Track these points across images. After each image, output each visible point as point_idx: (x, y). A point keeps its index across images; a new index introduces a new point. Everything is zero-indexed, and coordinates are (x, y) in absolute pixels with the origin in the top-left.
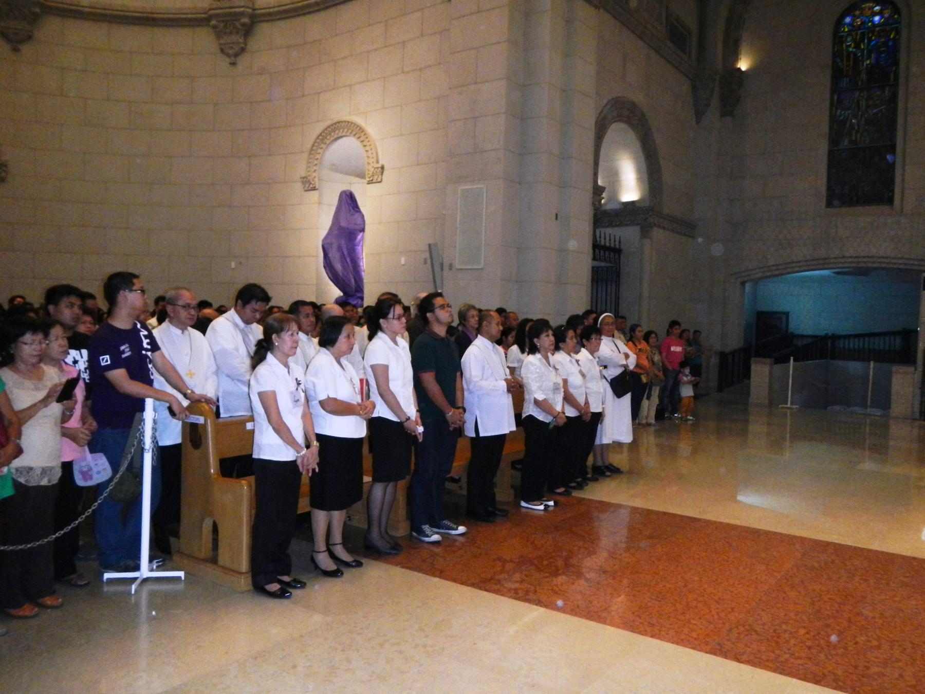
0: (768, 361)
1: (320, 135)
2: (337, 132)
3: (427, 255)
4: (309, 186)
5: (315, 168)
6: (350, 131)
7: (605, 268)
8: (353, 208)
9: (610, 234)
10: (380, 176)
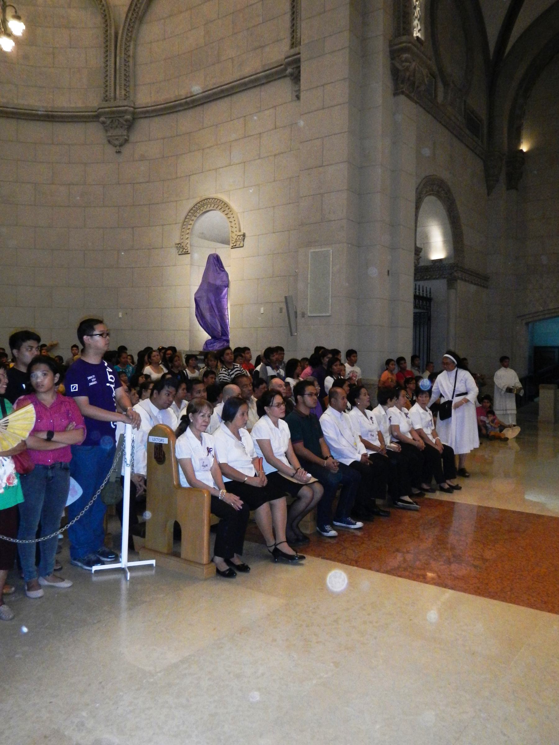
0: (552, 386)
1: (192, 209)
2: (205, 207)
3: (283, 306)
4: (183, 251)
5: (187, 236)
6: (216, 206)
7: (418, 314)
8: (220, 269)
9: (423, 286)
10: (242, 242)
